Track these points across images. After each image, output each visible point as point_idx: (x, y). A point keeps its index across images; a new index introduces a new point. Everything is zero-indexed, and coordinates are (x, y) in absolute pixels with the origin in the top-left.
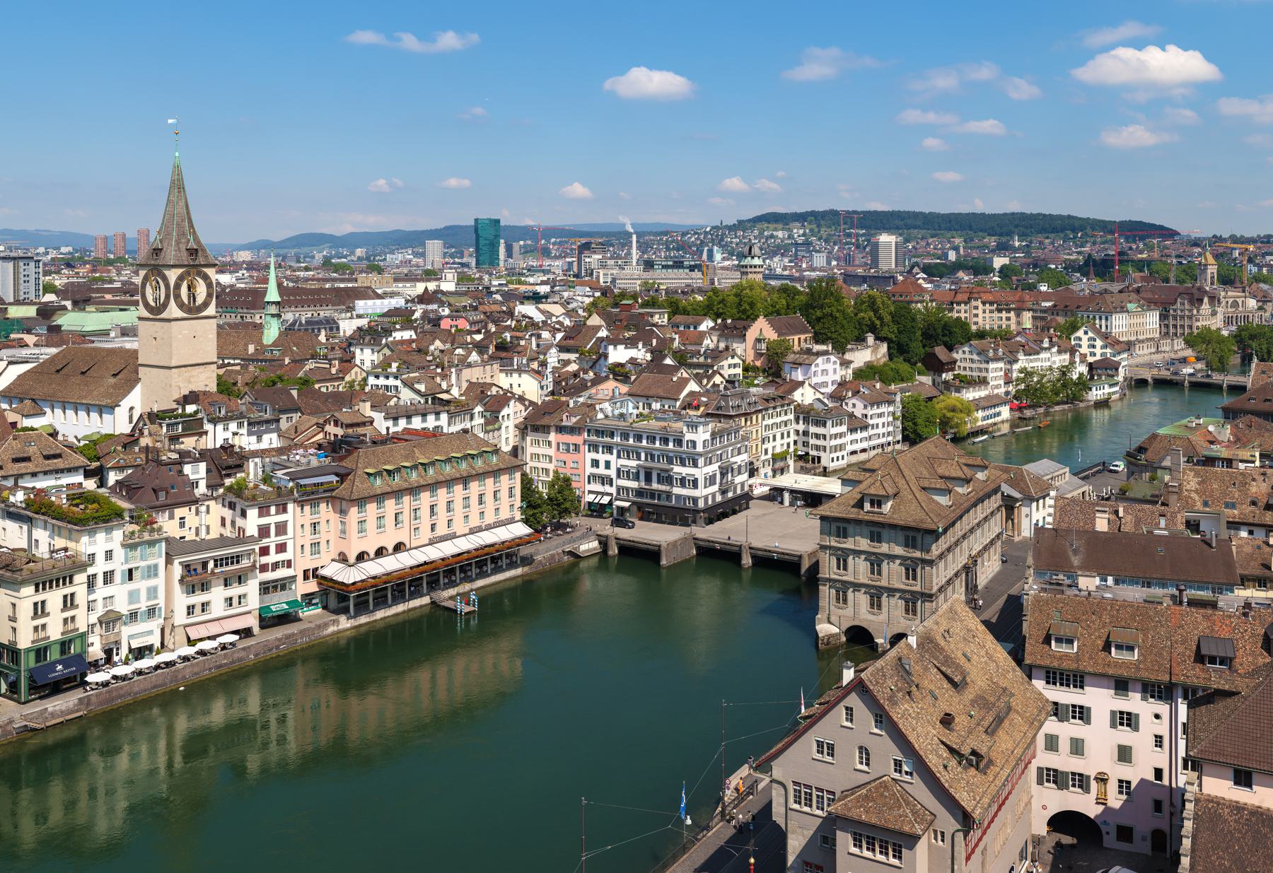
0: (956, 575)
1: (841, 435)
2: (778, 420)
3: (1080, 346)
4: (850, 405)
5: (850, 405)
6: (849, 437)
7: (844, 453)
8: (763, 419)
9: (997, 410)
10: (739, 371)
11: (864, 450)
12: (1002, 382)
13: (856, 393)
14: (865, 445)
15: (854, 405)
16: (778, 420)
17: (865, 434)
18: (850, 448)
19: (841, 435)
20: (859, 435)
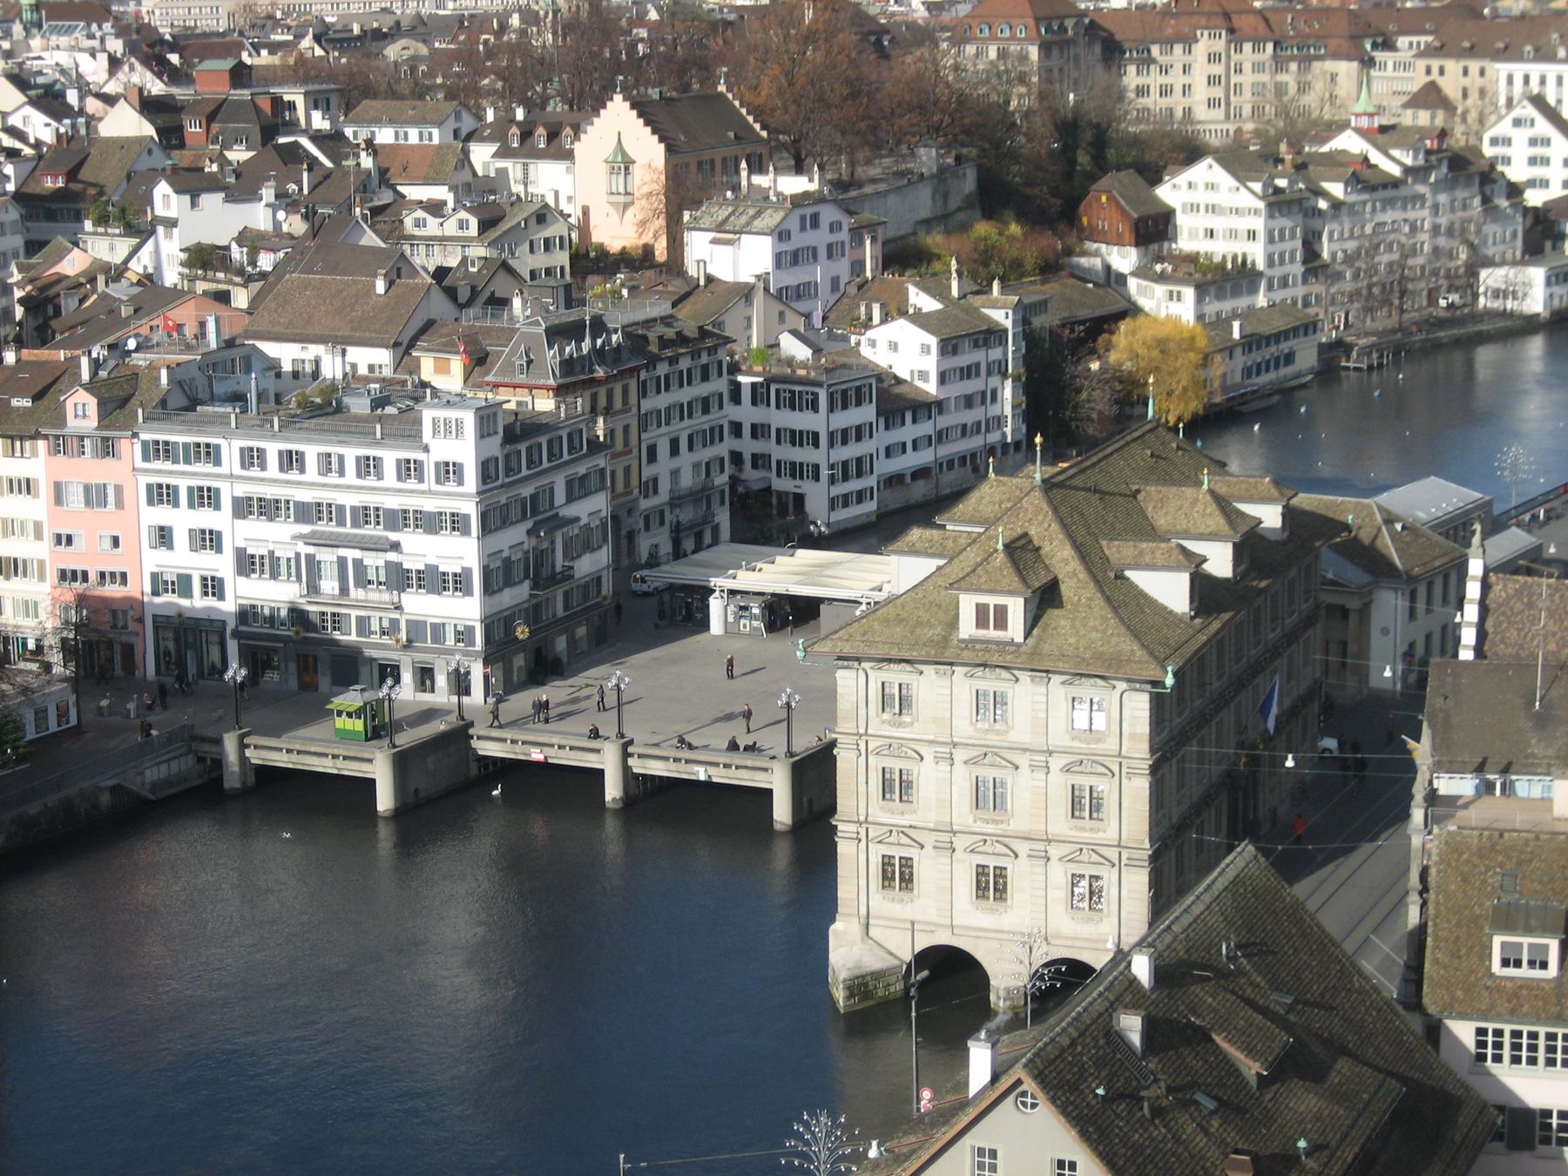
0: (1204, 802)
1: (860, 432)
2: (684, 395)
3: (1507, 161)
4: (882, 345)
5: (882, 345)
6: (883, 438)
7: (870, 481)
8: (643, 393)
9: (1285, 346)
10: (562, 258)
11: (921, 473)
12: (1298, 269)
13: (896, 309)
14: (925, 457)
15: (894, 347)
16: (684, 395)
17: (926, 428)
18: (885, 467)
19: (860, 432)
20: (908, 432)
